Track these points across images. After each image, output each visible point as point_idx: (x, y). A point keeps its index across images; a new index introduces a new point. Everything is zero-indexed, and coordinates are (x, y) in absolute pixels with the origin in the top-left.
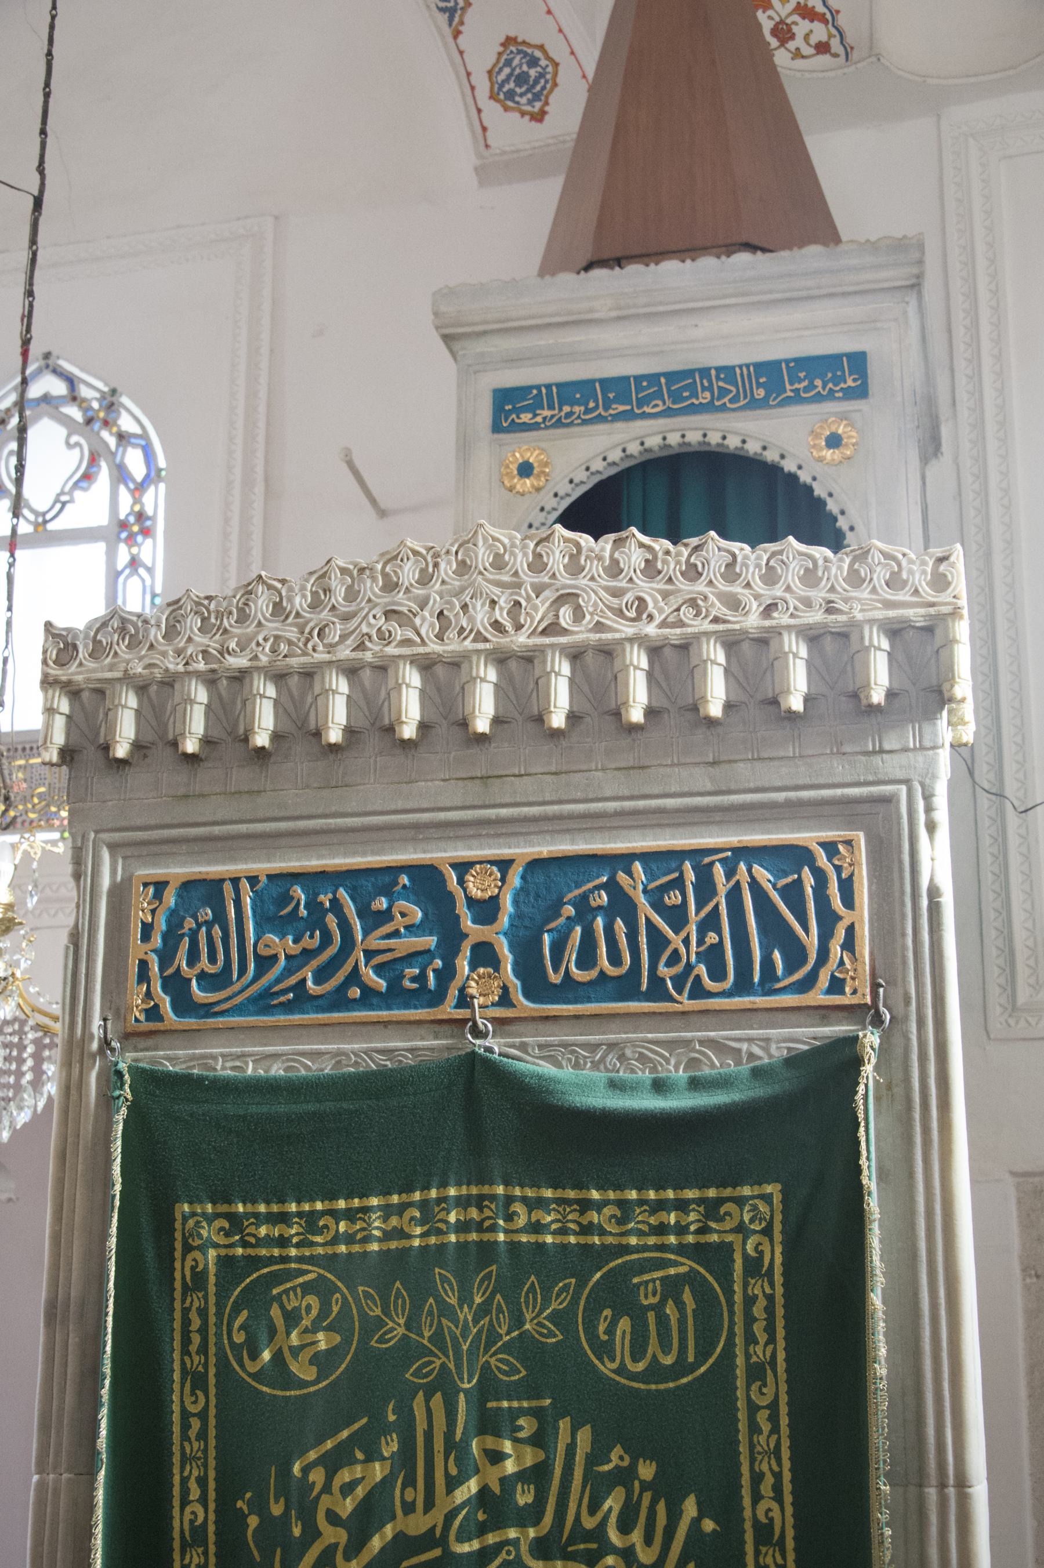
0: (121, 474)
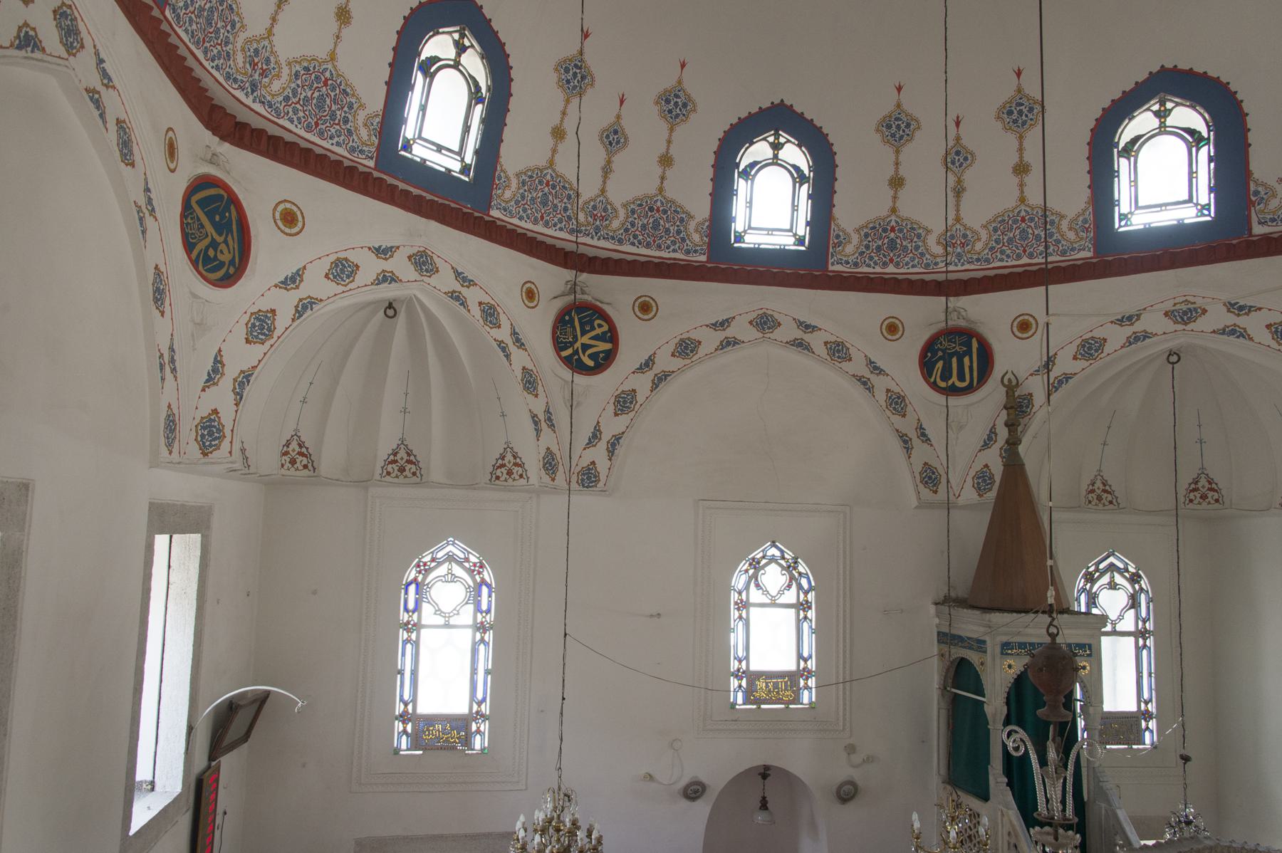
0: (800, 587)
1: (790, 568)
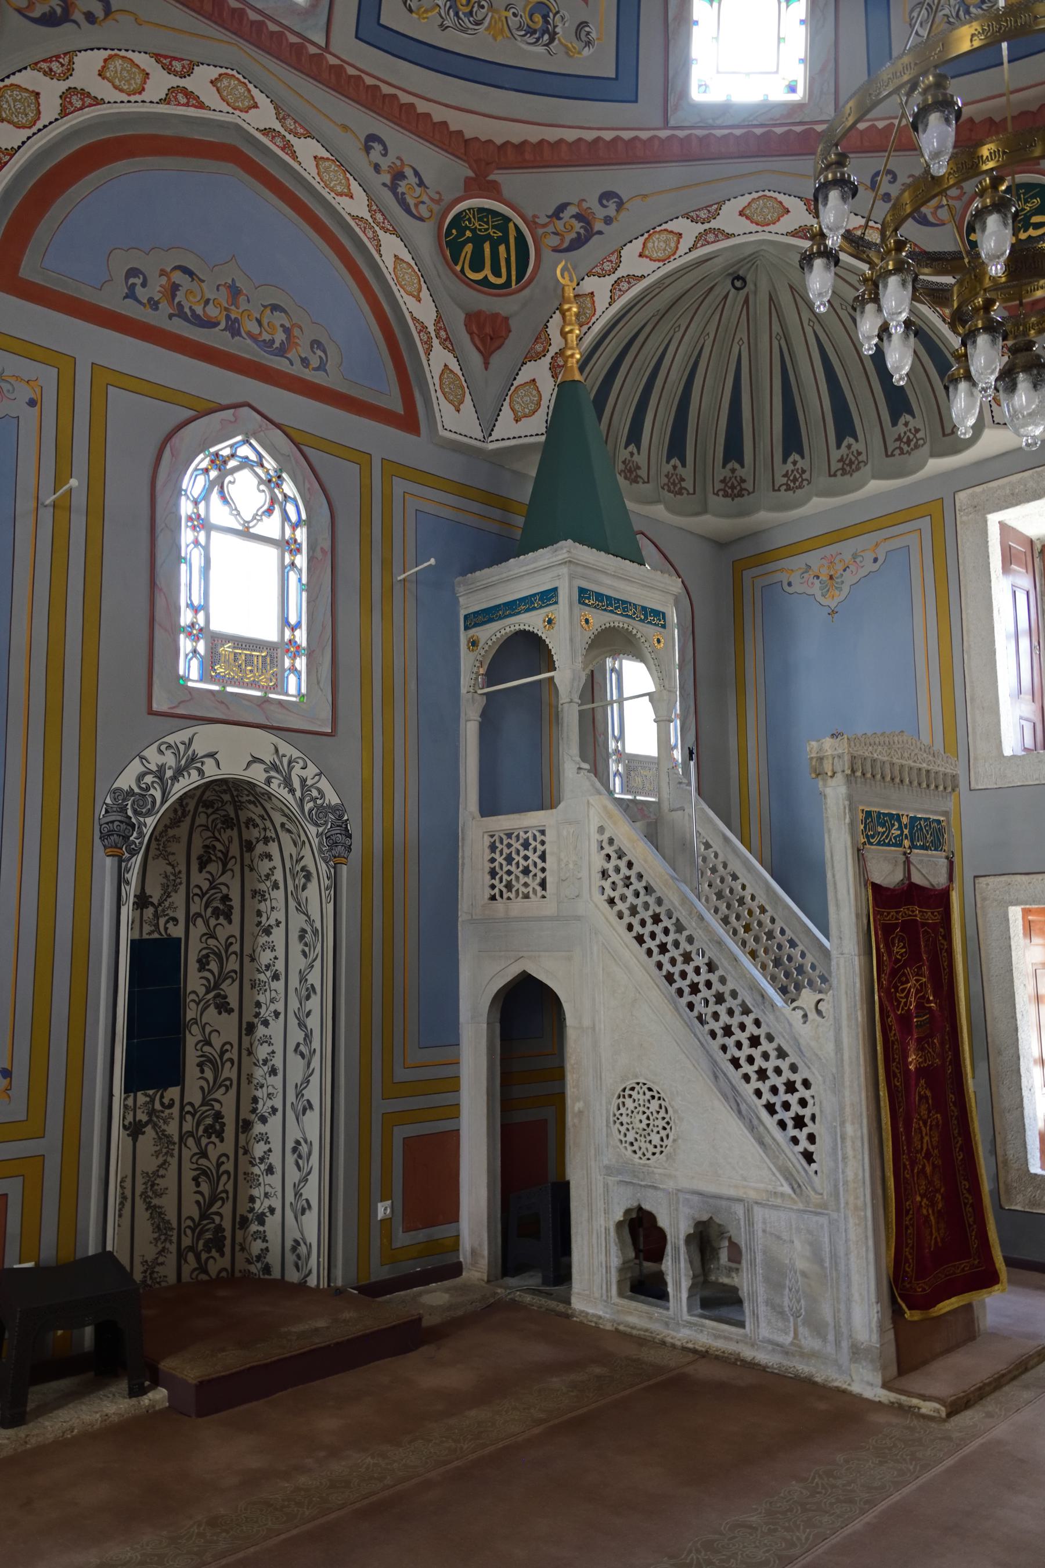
0: (285, 517)
1: (272, 482)
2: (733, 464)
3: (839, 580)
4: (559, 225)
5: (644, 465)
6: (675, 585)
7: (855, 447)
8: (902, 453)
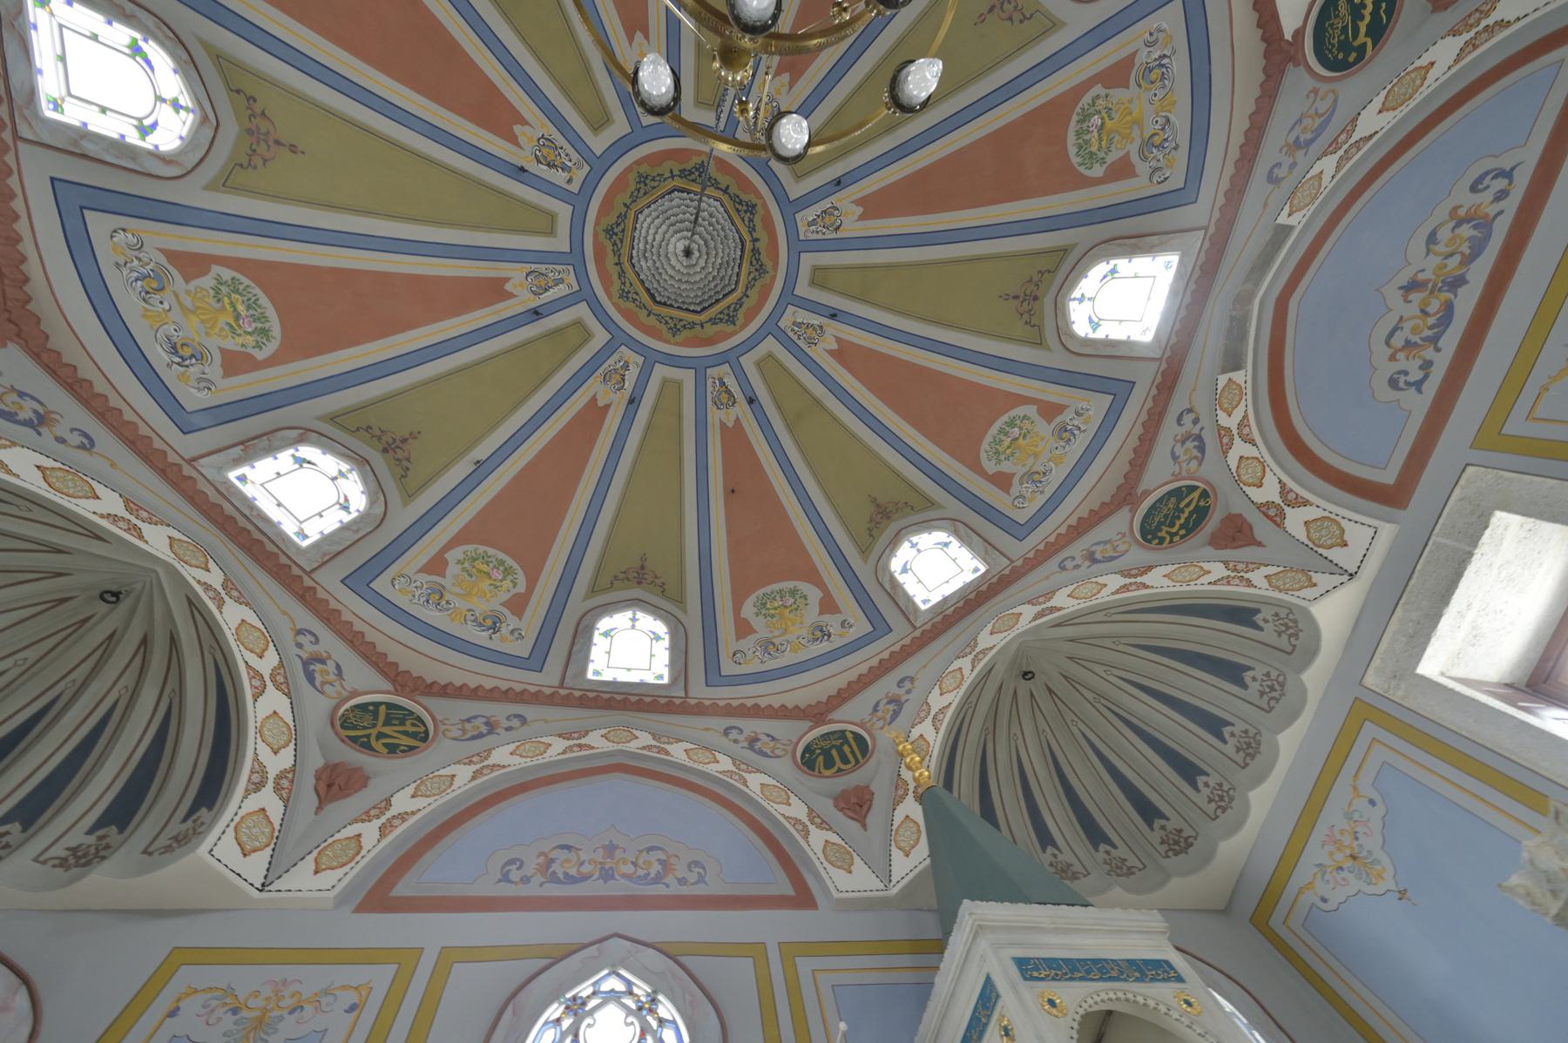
1: (643, 1010)
2: (1158, 823)
3: (1364, 853)
4: (879, 714)
5: (1073, 860)
6: (1156, 921)
7: (1236, 730)
8: (1277, 700)
